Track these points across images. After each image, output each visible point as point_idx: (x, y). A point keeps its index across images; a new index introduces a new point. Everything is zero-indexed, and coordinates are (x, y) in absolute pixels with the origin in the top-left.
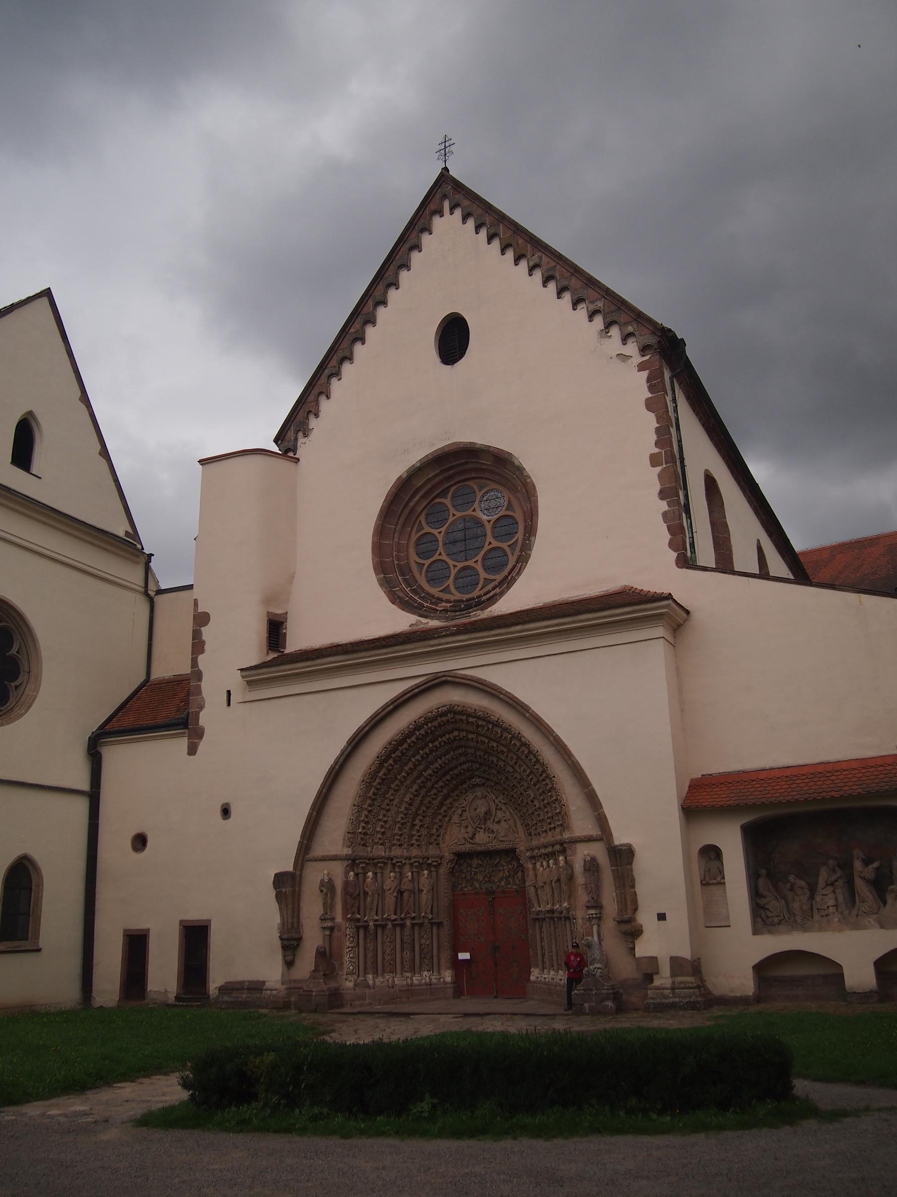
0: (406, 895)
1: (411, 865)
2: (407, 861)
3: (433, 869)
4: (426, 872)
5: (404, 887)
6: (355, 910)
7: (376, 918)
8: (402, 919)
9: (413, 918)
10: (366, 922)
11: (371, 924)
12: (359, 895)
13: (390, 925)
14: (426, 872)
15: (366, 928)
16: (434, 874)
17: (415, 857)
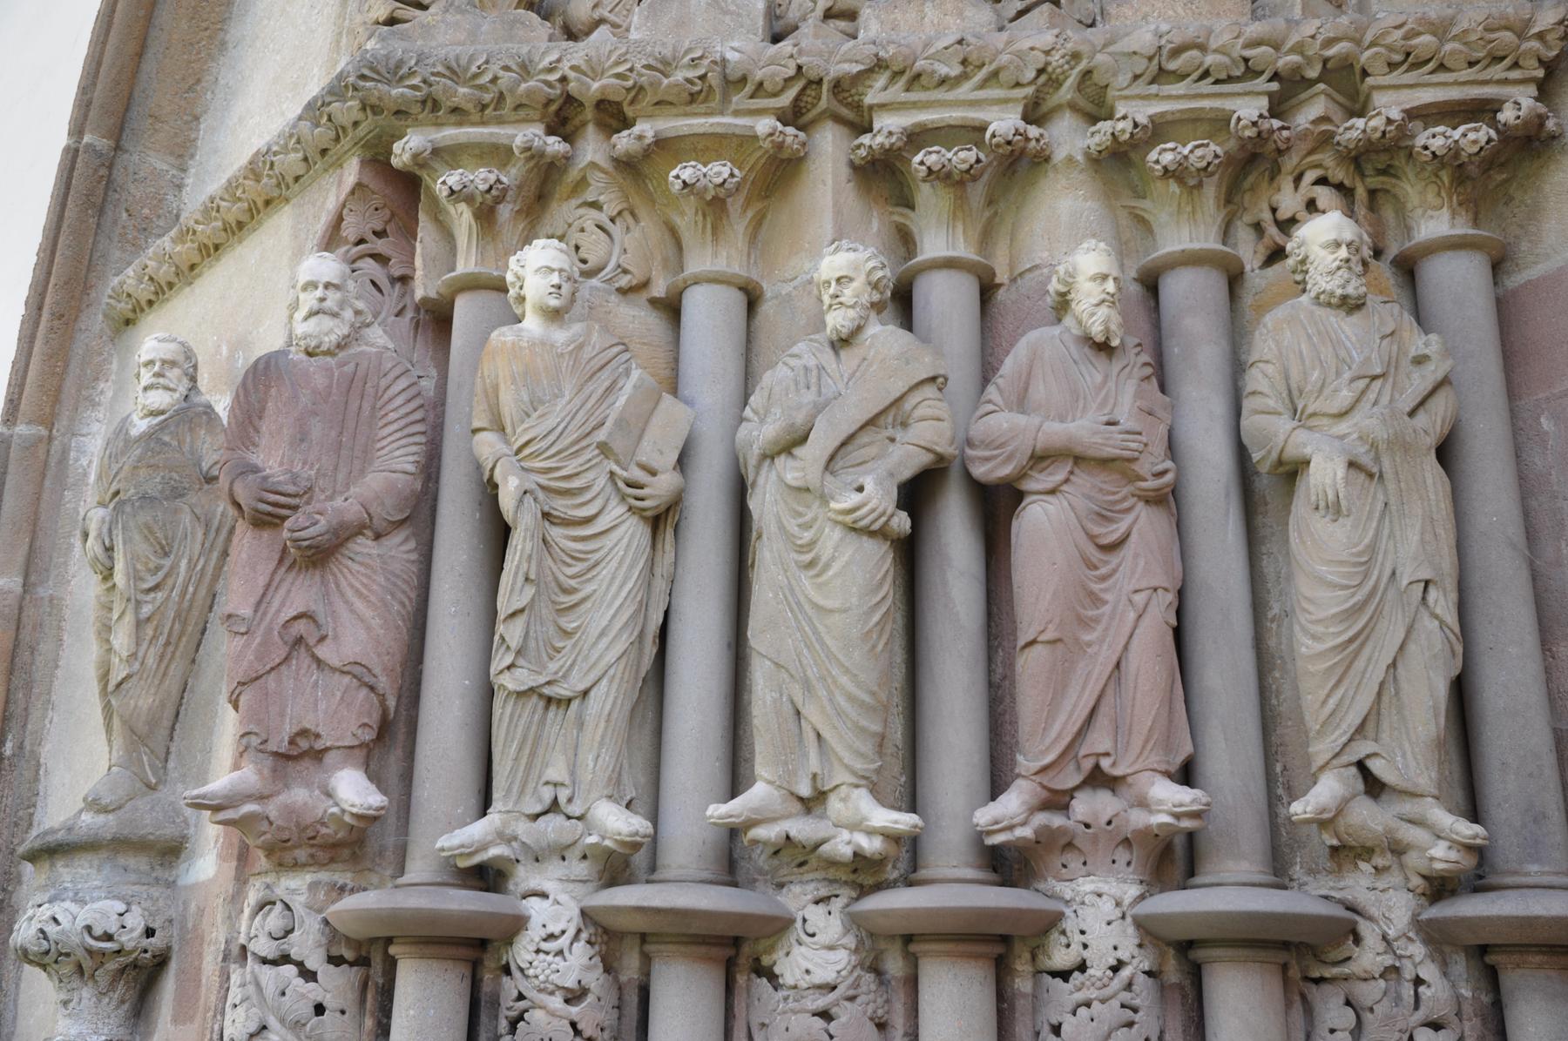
0: (1041, 523)
1: (1118, 162)
2: (1069, 138)
3: (1435, 222)
4: (1325, 236)
5: (1004, 432)
6: (339, 714)
7: (616, 822)
8: (1005, 863)
9: (1175, 857)
10: (487, 876)
11: (552, 907)
12: (419, 513)
13: (818, 951)
14: (1325, 236)
15: (478, 952)
16: (1458, 281)
17: (1160, 71)
